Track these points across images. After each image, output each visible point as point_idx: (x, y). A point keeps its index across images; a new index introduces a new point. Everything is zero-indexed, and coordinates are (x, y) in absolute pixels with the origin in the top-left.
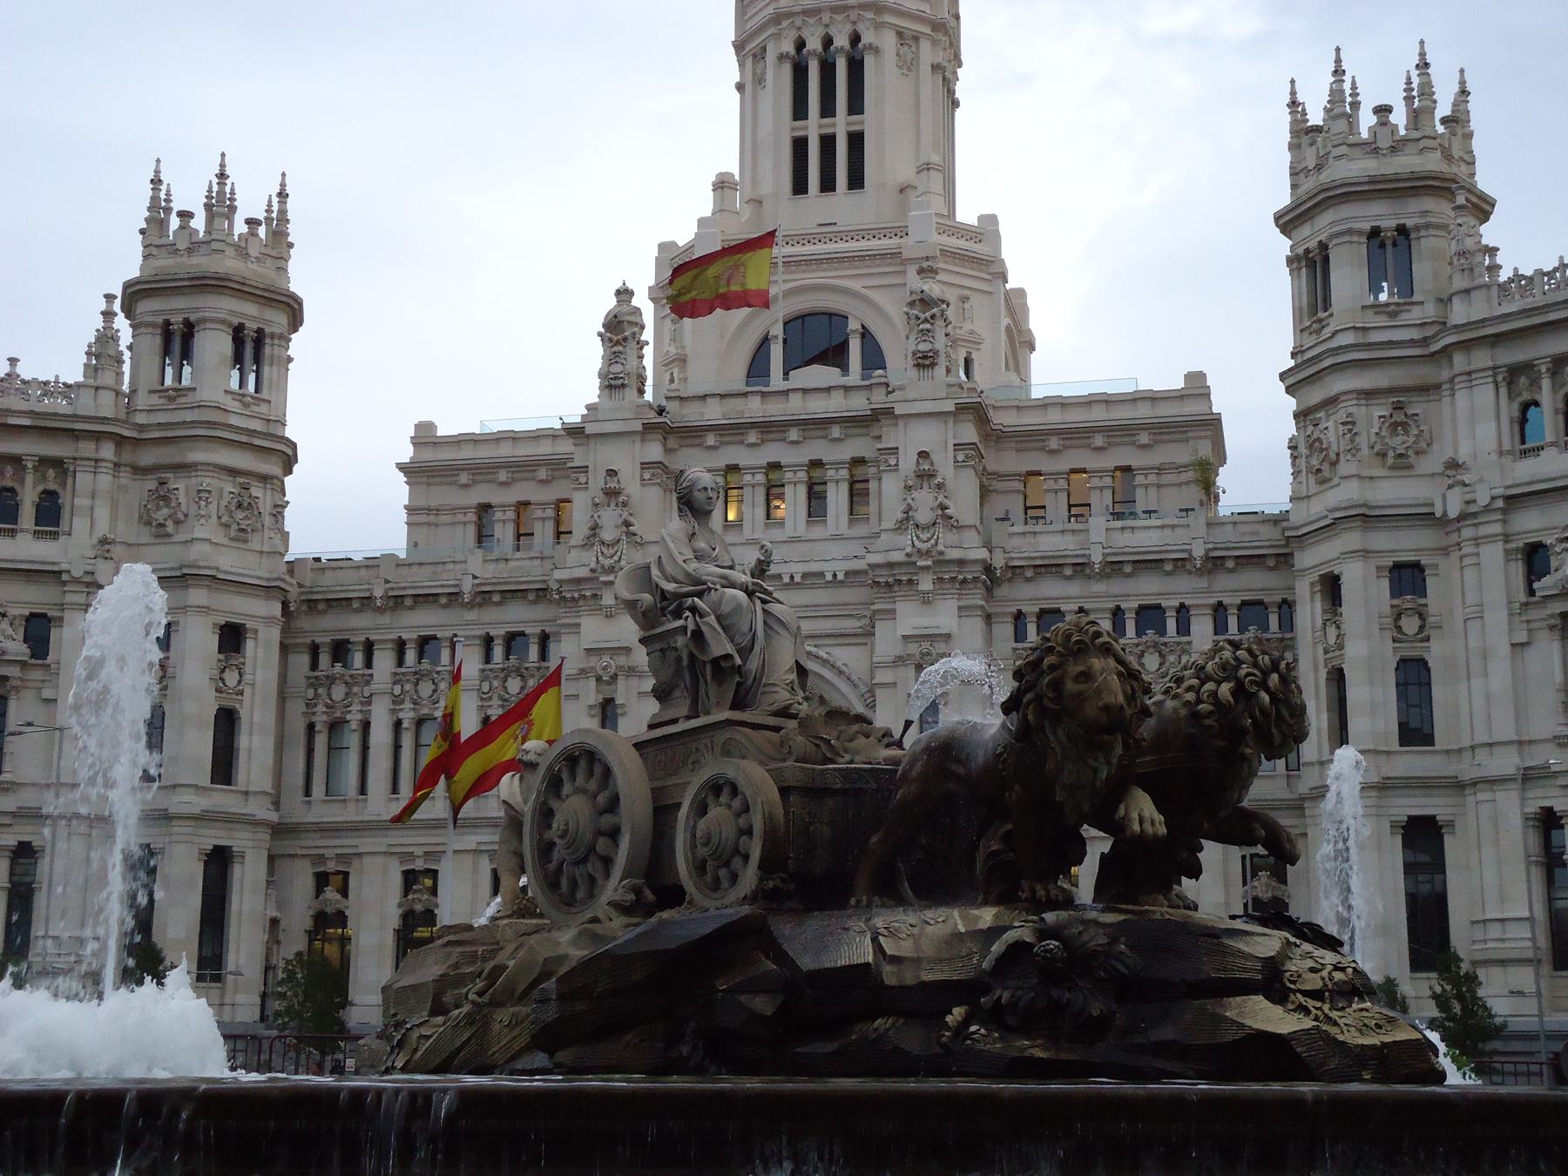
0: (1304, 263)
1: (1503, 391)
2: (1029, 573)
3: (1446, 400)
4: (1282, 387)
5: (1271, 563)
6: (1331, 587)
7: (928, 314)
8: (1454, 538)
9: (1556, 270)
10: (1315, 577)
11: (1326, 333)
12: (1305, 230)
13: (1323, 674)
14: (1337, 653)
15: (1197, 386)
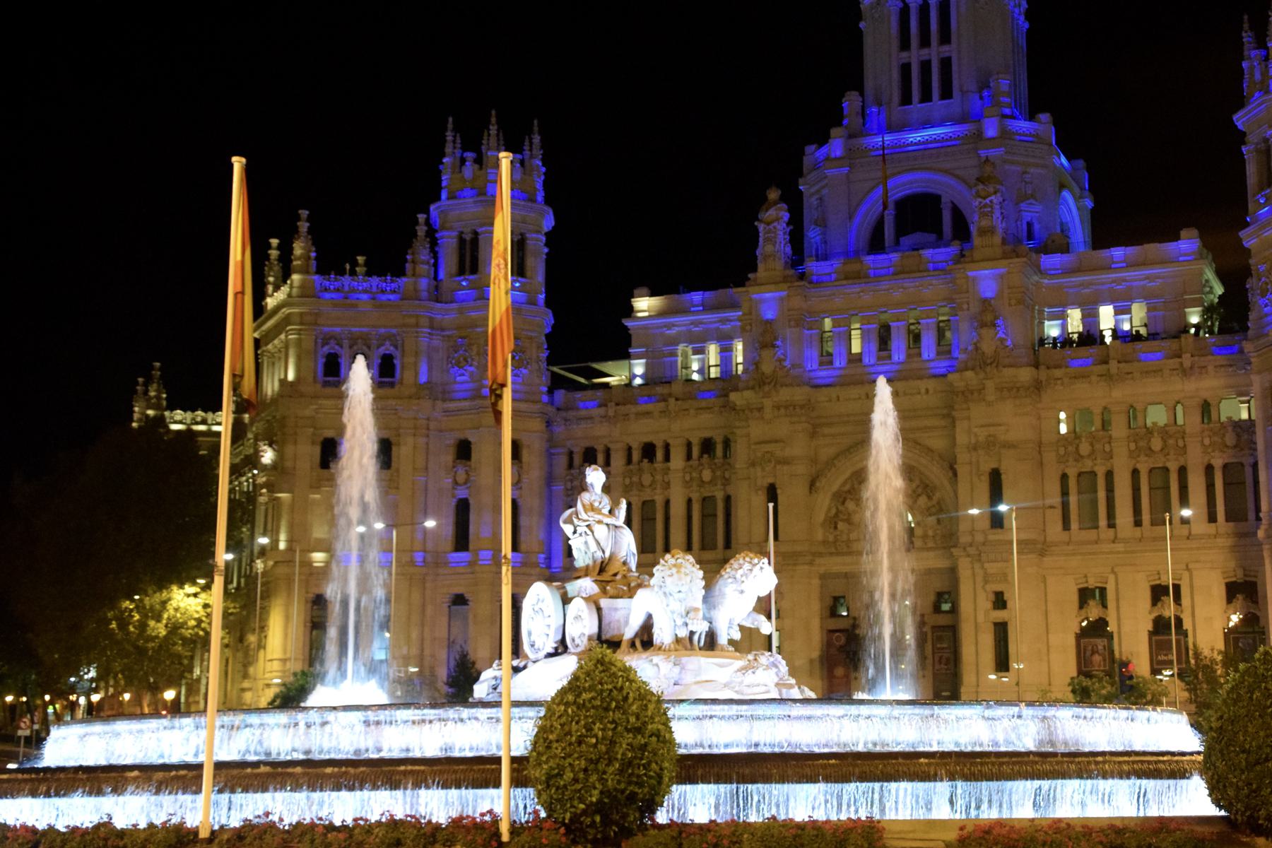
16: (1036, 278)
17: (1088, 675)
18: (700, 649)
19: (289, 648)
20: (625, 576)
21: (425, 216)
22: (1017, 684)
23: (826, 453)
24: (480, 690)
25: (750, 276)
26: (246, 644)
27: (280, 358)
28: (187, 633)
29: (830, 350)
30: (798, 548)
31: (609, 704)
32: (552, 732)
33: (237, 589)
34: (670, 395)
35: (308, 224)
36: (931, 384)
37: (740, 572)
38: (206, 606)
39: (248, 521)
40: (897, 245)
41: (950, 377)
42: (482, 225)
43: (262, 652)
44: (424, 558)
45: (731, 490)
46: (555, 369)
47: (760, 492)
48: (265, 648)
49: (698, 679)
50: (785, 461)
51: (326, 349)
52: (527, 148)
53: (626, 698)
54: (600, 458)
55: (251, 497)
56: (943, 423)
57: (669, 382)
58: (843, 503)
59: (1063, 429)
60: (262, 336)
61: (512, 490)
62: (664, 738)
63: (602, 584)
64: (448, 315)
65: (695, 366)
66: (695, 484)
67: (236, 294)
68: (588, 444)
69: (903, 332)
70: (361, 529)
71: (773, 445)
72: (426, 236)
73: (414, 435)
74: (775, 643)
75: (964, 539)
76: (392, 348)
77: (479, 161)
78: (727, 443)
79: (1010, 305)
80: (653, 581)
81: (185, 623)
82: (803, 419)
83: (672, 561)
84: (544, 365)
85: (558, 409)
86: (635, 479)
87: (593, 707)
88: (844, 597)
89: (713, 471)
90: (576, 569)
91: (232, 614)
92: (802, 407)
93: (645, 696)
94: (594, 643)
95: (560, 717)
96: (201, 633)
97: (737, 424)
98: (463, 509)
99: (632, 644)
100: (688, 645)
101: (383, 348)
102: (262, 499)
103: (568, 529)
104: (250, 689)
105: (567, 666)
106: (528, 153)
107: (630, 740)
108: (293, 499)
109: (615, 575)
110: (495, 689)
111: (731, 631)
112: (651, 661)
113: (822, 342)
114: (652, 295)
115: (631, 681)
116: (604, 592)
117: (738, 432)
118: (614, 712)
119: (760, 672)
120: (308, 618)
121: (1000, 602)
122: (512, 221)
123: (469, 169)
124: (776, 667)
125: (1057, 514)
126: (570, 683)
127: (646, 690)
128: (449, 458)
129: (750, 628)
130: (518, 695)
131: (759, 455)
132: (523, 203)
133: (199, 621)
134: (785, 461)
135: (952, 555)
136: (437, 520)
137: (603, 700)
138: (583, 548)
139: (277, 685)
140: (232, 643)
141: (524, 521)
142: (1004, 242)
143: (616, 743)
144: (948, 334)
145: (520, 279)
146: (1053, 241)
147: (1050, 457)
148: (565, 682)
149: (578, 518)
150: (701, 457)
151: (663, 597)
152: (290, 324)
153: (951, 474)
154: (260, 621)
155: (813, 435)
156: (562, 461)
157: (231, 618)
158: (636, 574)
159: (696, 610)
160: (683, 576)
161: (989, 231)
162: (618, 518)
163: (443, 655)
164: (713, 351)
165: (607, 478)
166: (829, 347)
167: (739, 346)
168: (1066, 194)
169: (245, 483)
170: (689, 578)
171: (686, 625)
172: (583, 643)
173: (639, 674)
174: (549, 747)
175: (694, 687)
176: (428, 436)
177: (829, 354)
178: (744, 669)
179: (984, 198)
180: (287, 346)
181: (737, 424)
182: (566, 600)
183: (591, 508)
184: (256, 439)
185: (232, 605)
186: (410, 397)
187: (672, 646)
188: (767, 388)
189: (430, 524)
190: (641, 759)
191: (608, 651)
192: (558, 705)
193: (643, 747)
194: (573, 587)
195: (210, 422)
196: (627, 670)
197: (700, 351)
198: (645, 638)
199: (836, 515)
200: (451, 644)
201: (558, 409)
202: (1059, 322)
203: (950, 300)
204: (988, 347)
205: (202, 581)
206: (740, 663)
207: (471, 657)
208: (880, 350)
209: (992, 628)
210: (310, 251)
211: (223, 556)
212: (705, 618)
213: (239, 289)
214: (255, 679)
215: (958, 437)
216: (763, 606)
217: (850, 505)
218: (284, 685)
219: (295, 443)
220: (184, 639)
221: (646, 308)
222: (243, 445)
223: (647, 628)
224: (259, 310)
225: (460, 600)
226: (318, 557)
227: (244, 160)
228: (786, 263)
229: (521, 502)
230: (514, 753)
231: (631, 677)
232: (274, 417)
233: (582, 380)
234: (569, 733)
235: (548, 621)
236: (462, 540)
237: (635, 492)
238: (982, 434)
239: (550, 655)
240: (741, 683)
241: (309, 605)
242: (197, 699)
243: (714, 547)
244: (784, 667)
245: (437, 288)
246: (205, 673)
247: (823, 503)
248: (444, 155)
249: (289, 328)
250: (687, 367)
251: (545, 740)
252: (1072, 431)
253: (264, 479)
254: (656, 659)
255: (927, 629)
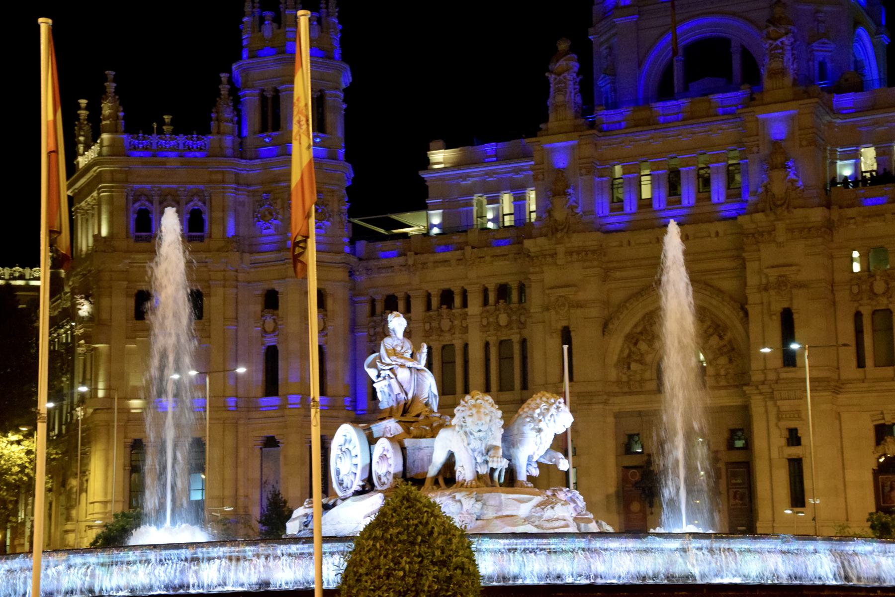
16: (828, 118)
17: (888, 511)
18: (501, 485)
19: (109, 490)
20: (427, 417)
21: (228, 75)
22: (814, 519)
23: (618, 297)
24: (292, 527)
25: (541, 126)
26: (68, 488)
27: (93, 215)
28: (11, 479)
29: (621, 196)
30: (591, 388)
31: (415, 538)
32: (361, 566)
33: (59, 435)
34: (466, 243)
35: (115, 85)
36: (721, 227)
37: (538, 411)
38: (29, 452)
39: (67, 371)
40: (686, 92)
41: (742, 219)
42: (282, 83)
43: (84, 495)
44: (236, 402)
45: (526, 333)
46: (356, 221)
47: (554, 335)
48: (86, 492)
49: (500, 514)
50: (579, 305)
51: (137, 205)
52: (323, 6)
53: (431, 533)
54: (401, 305)
55: (70, 349)
56: (734, 264)
57: (466, 231)
58: (636, 344)
59: (857, 267)
60: (75, 194)
61: (319, 337)
62: (469, 569)
63: (405, 424)
64: (253, 170)
65: (490, 215)
66: (492, 329)
67: (49, 153)
68: (390, 292)
69: (693, 176)
70: (176, 377)
71: (568, 289)
72: (229, 95)
73: (224, 287)
74: (572, 480)
75: (757, 377)
76: (200, 204)
77: (278, 20)
78: (522, 289)
79: (801, 146)
80: (454, 421)
81: (9, 469)
82: (595, 263)
83: (473, 402)
84: (345, 218)
85: (360, 259)
86: (435, 324)
87: (400, 542)
88: (638, 435)
89: (509, 316)
90: (381, 411)
91: (54, 459)
92: (594, 252)
93: (448, 529)
94: (400, 481)
95: (369, 551)
96: (25, 478)
97: (531, 270)
98: (271, 357)
99: (436, 481)
100: (490, 483)
101: (192, 204)
102: (80, 350)
103: (372, 373)
104: (72, 531)
105: (374, 502)
106: (324, 10)
107: (436, 573)
108: (110, 348)
109: (418, 416)
110: (306, 526)
111: (530, 468)
112: (454, 497)
113: (612, 189)
114: (447, 147)
115: (436, 517)
116: (408, 432)
117: (533, 277)
118: (420, 546)
119: (558, 507)
120: (128, 462)
122: (311, 78)
123: (268, 29)
124: (574, 502)
125: (852, 349)
126: (377, 518)
127: (449, 525)
128: (257, 307)
129: (548, 465)
130: (328, 531)
131: (553, 299)
132: (321, 60)
133: (23, 467)
134: (579, 305)
135: (744, 394)
136: (245, 366)
137: (409, 534)
138: (386, 390)
139: (99, 526)
140: (54, 488)
141: (329, 367)
142: (795, 83)
143: (422, 575)
144: (738, 178)
145: (320, 134)
146: (846, 80)
147: (843, 296)
148: (373, 518)
149: (381, 362)
150: (497, 302)
151: (464, 437)
152: (101, 183)
153: (741, 314)
154: (81, 466)
155: (605, 278)
156: (365, 309)
157: (54, 463)
158: (438, 415)
159: (496, 448)
160: (483, 416)
161: (782, 72)
162: (419, 362)
163: (256, 495)
164: (507, 201)
165: (408, 324)
166: (620, 193)
167: (532, 196)
168: (861, 31)
169: (64, 334)
170: (488, 418)
171: (487, 462)
172: (388, 481)
173: (443, 510)
174: (358, 581)
175: (497, 522)
176: (237, 287)
177: (620, 201)
178: (542, 505)
179: (775, 40)
180: (99, 203)
181: (531, 270)
182: (372, 441)
183: (394, 353)
184: (73, 293)
185: (54, 451)
186: (219, 250)
187: (474, 483)
188: (559, 235)
189: (241, 370)
190: (447, 591)
191: (413, 488)
192: (367, 539)
193: (449, 579)
194: (377, 428)
195: (27, 277)
196: (433, 506)
197: (494, 200)
198: (448, 476)
199: (629, 356)
200: (263, 484)
201: (360, 259)
202: (852, 161)
203: (740, 144)
204: (778, 189)
205: (24, 429)
206: (538, 499)
207: (283, 495)
208: (670, 195)
209: (786, 463)
210: (118, 111)
211: (45, 405)
212: (504, 456)
213: (52, 148)
214: (78, 521)
215: (748, 279)
216: (560, 443)
217: (643, 346)
218: (105, 526)
219: (110, 296)
220: (8, 484)
221: (441, 160)
222: (60, 298)
223: (450, 464)
224: (71, 168)
225: (271, 442)
226: (136, 404)
227: (50, 21)
228: (576, 111)
229: (328, 350)
230: (325, 586)
231: (436, 512)
232: (90, 271)
233: (382, 231)
234: (378, 567)
235: (355, 461)
236: (271, 385)
237: (434, 337)
238: (773, 274)
239: (357, 493)
240: (541, 517)
241: (128, 450)
242: (22, 541)
243: (511, 389)
244: (581, 503)
245: (241, 144)
246: (29, 516)
247: (616, 344)
248: (243, 14)
249: (100, 186)
250: (482, 216)
251: (355, 573)
252: (866, 268)
253: (82, 331)
254: (458, 496)
255: (721, 465)
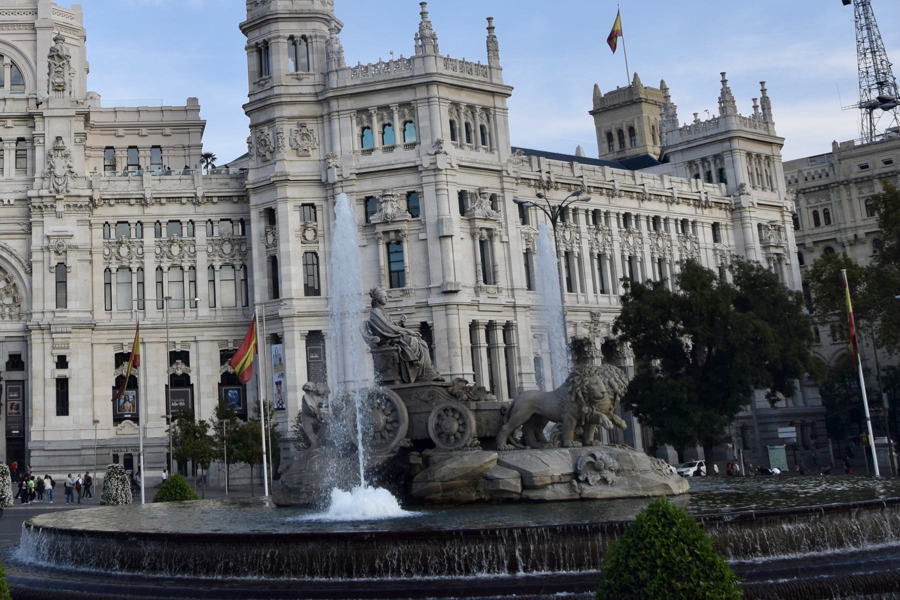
0: (255, 49)
1: (354, 121)
2: (112, 202)
3: (326, 124)
4: (243, 111)
5: (235, 200)
6: (270, 215)
7: (61, 63)
8: (330, 193)
9: (378, 64)
10: (262, 209)
11: (267, 86)
12: (256, 33)
13: (265, 258)
14: (273, 248)
15: (193, 105)
121: (62, 362)
